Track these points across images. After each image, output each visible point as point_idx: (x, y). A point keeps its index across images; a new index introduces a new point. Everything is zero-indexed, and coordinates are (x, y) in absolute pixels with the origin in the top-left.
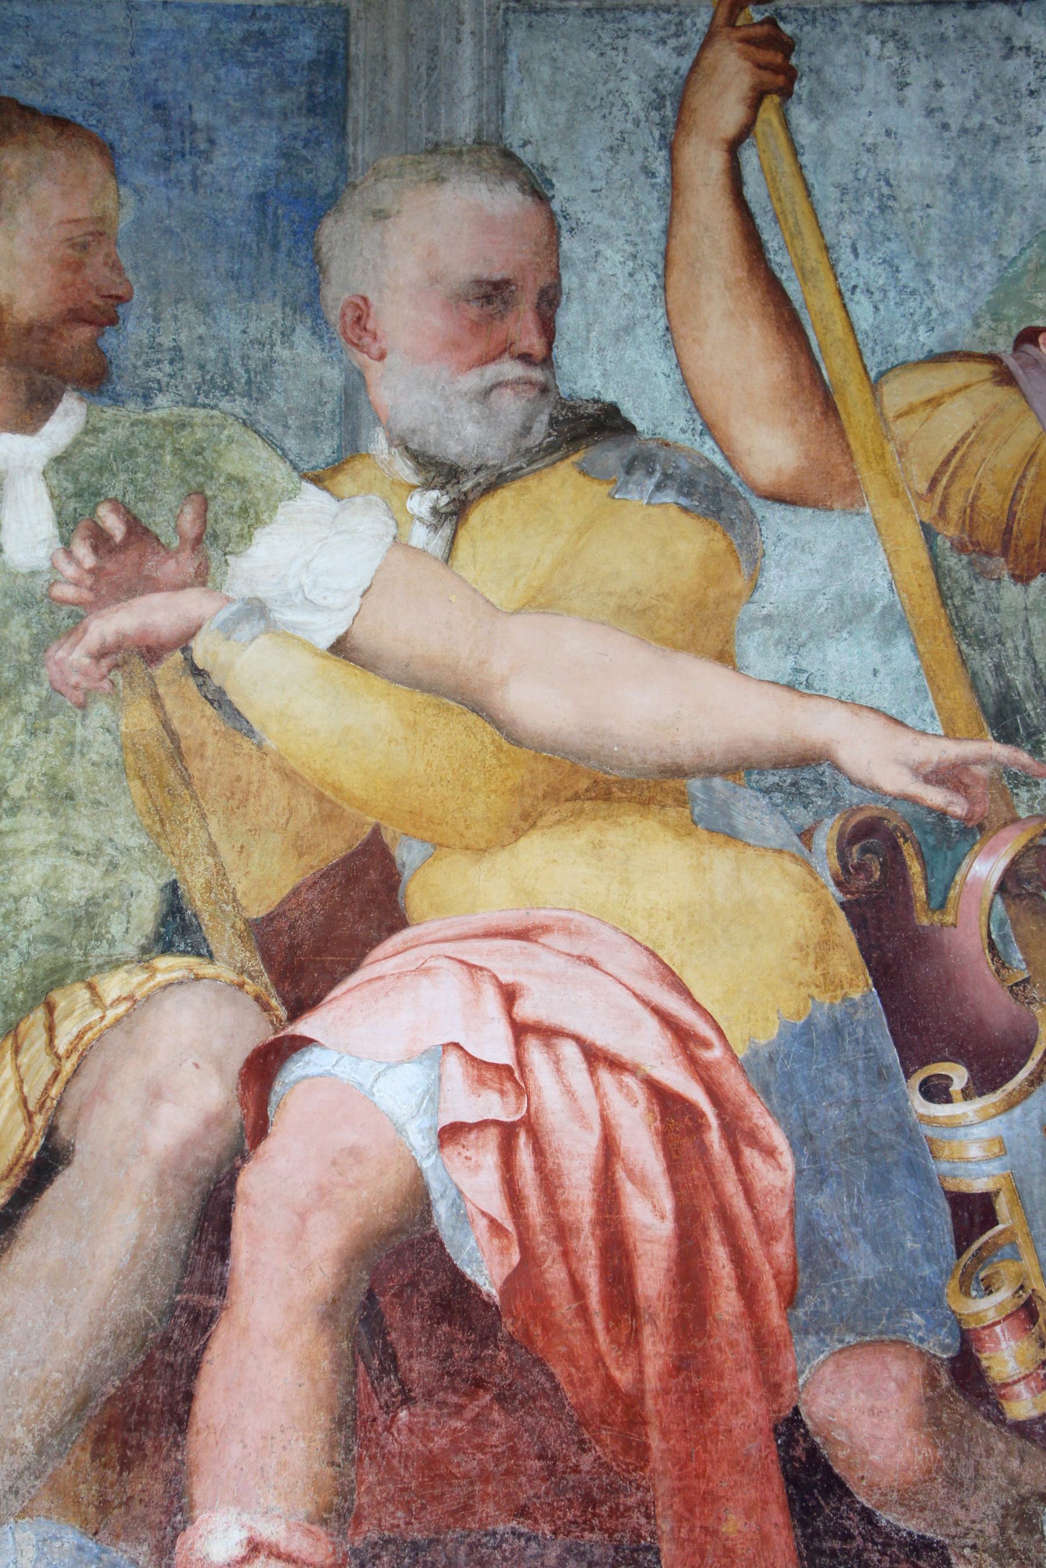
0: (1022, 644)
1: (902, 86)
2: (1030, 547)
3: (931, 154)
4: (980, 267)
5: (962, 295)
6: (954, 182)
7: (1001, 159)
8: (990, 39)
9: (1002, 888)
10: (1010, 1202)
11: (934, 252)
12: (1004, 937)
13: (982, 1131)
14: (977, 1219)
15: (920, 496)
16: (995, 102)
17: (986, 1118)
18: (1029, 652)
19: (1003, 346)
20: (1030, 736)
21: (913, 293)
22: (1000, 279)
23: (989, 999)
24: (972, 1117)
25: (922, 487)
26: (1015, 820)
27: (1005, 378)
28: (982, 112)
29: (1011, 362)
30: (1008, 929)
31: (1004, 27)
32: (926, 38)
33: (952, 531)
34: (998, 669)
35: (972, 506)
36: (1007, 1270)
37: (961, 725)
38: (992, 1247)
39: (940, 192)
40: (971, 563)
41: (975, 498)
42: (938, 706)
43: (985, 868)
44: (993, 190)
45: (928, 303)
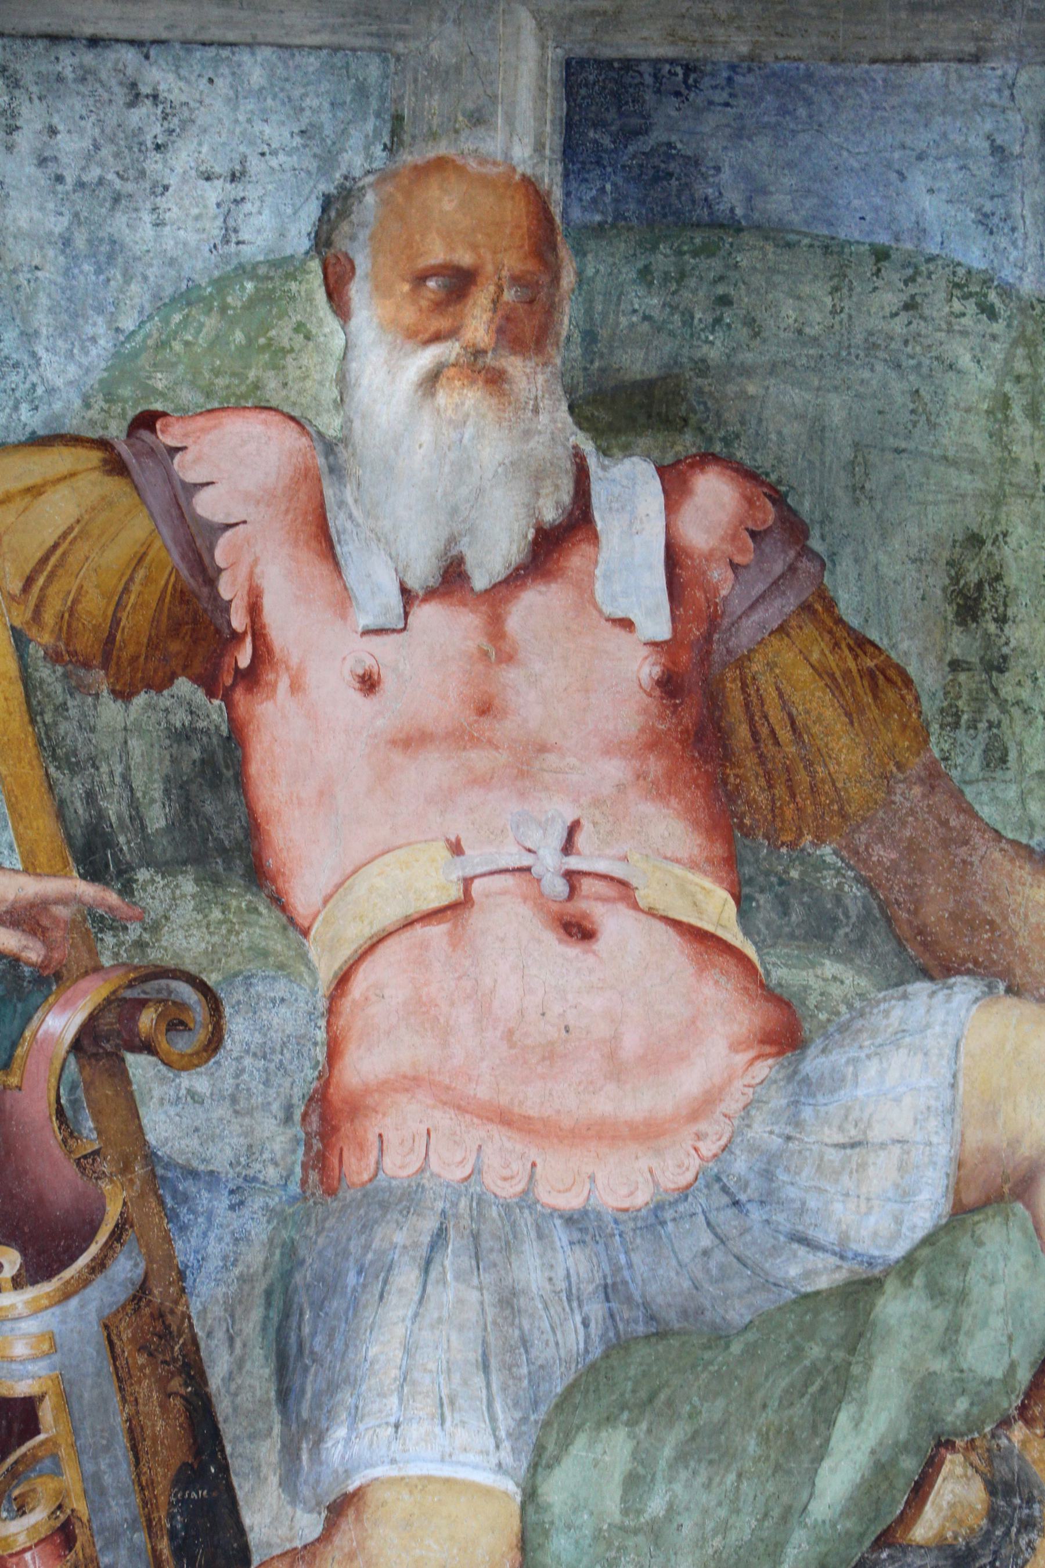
0: (119, 769)
1: (11, 129)
2: (134, 659)
3: (42, 208)
4: (94, 340)
5: (72, 371)
6: (67, 242)
7: (121, 219)
8: (113, 82)
9: (76, 1046)
10: (55, 1408)
11: (42, 320)
12: (74, 1103)
13: (31, 1326)
14: (16, 1427)
15: (13, 598)
16: (117, 155)
17: (37, 1311)
18: (126, 778)
19: (116, 430)
20: (120, 873)
21: (16, 365)
22: (116, 355)
23: (54, 1174)
24: (21, 1309)
25: (15, 586)
26: (98, 969)
27: (116, 466)
28: (102, 164)
29: (123, 449)
30: (80, 1093)
31: (129, 71)
32: (41, 78)
33: (46, 638)
34: (90, 797)
35: (71, 611)
36: (45, 1487)
37: (42, 858)
38: (31, 1461)
39: (51, 253)
40: (66, 676)
41: (76, 601)
42: (19, 837)
43: (60, 1023)
44: (110, 253)
45: (34, 378)
